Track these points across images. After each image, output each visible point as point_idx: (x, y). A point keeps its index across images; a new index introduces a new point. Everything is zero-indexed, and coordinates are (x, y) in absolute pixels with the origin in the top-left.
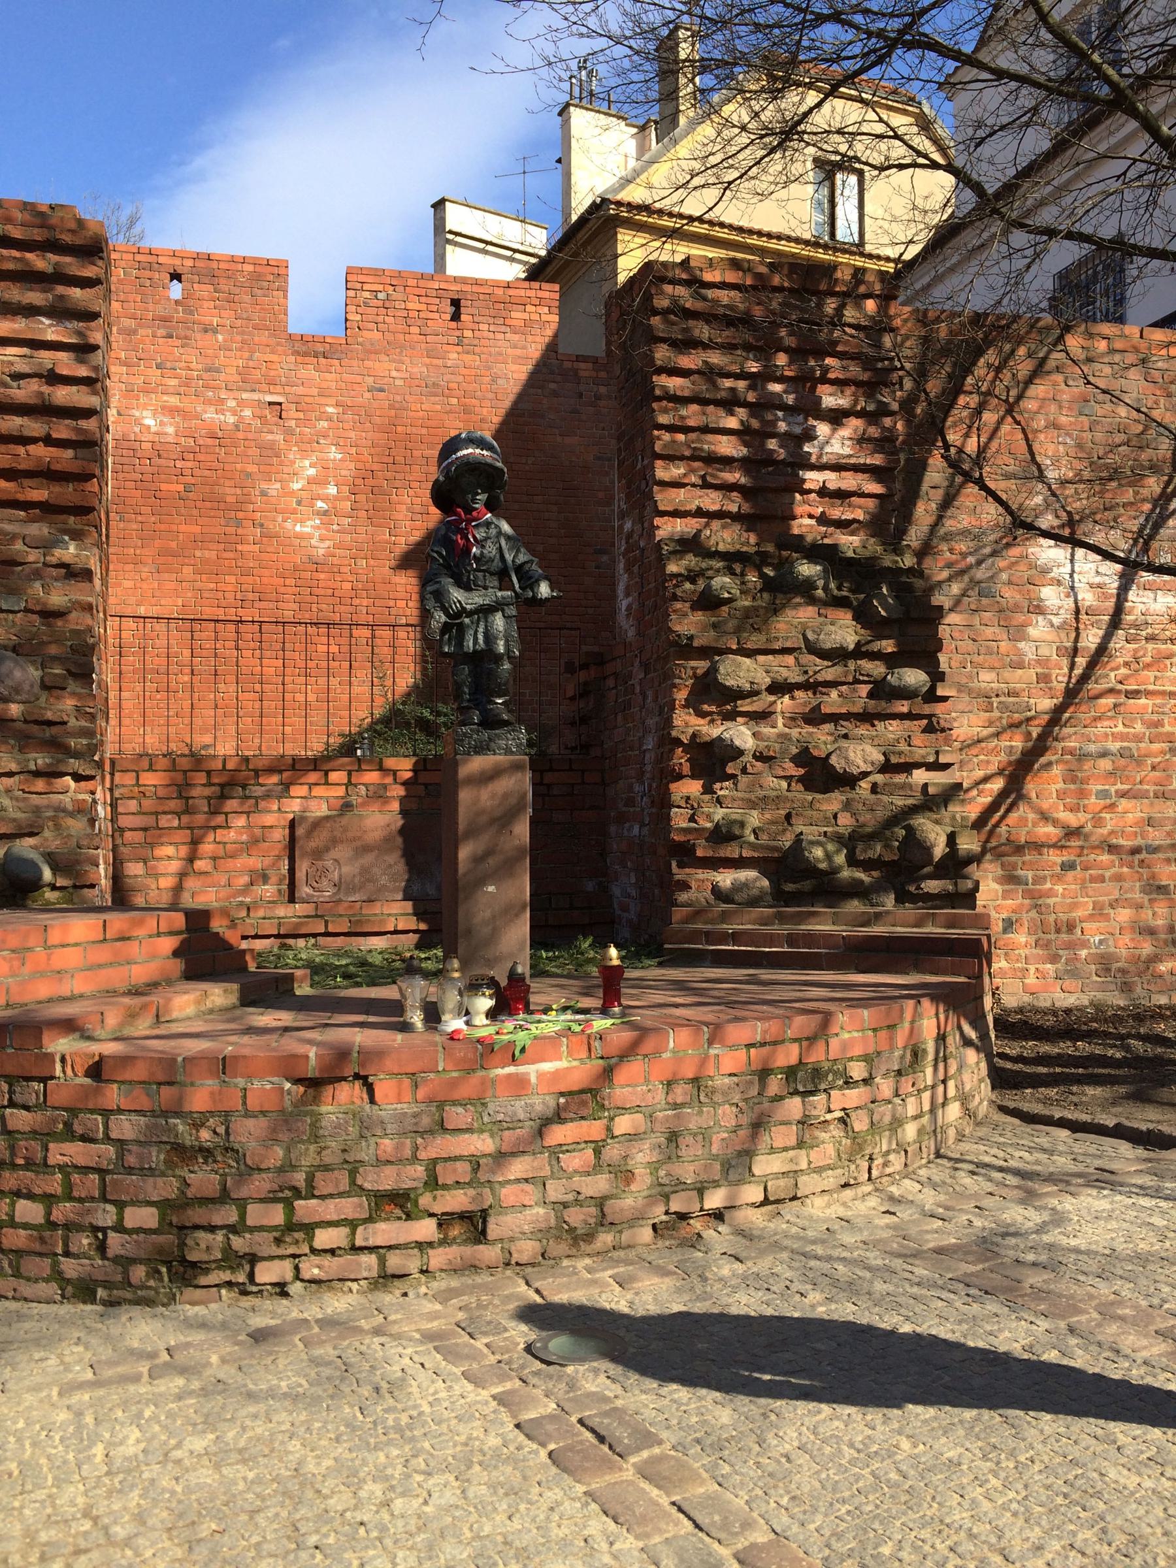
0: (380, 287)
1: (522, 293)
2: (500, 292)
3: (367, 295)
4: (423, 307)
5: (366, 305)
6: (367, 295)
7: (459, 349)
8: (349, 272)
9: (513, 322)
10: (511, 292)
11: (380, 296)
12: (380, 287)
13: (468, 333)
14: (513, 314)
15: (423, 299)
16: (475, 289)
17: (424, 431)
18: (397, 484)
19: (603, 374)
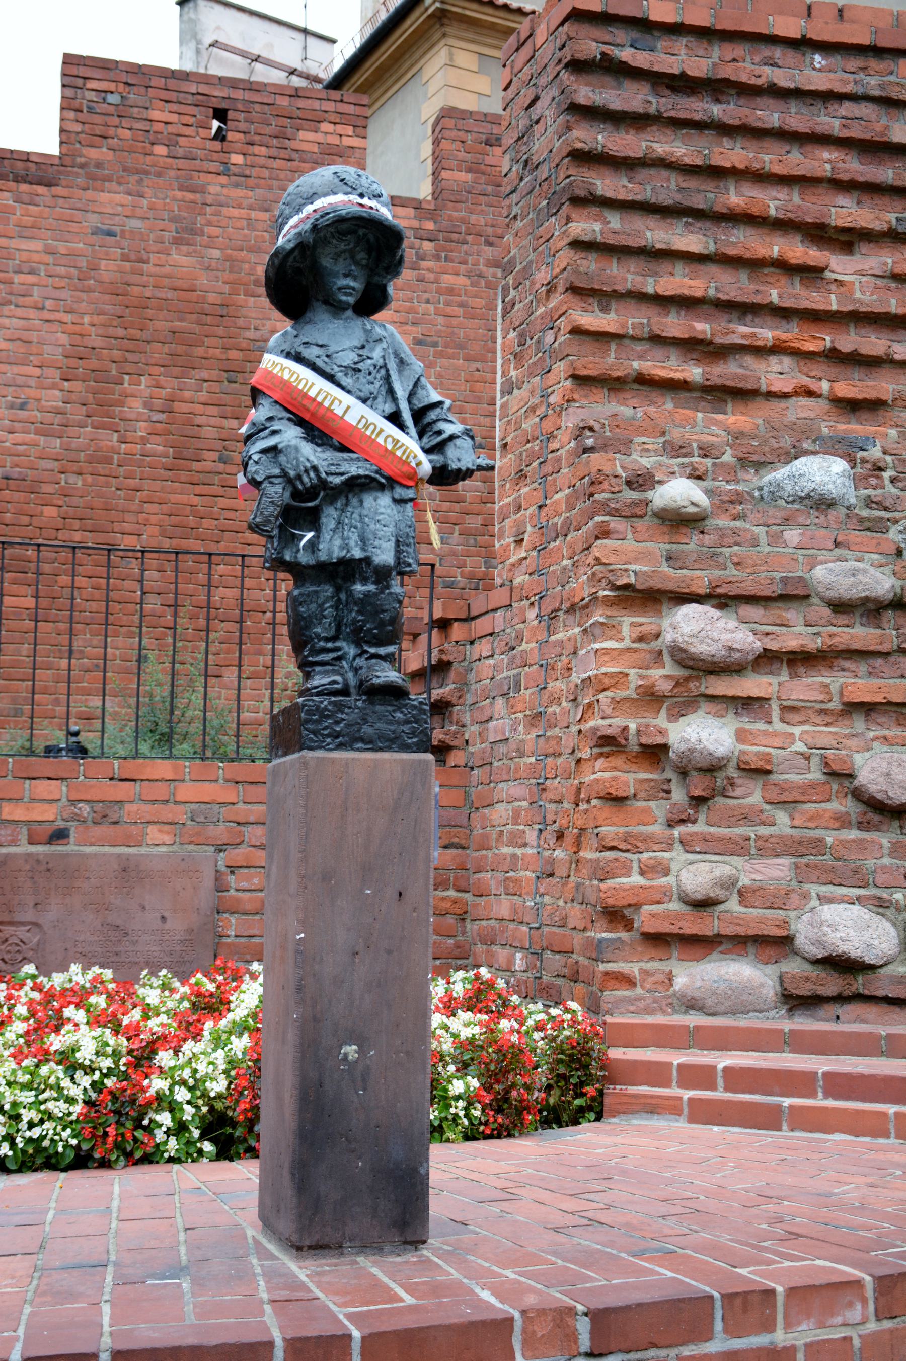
0: (112, 86)
1: (316, 105)
2: (284, 102)
3: (92, 96)
4: (174, 118)
5: (90, 110)
6: (92, 96)
7: (223, 179)
8: (69, 61)
9: (305, 146)
10: (301, 103)
11: (113, 99)
12: (112, 86)
13: (237, 159)
14: (302, 134)
15: (175, 107)
16: (247, 95)
17: (170, 294)
18: (129, 368)
19: (430, 225)
